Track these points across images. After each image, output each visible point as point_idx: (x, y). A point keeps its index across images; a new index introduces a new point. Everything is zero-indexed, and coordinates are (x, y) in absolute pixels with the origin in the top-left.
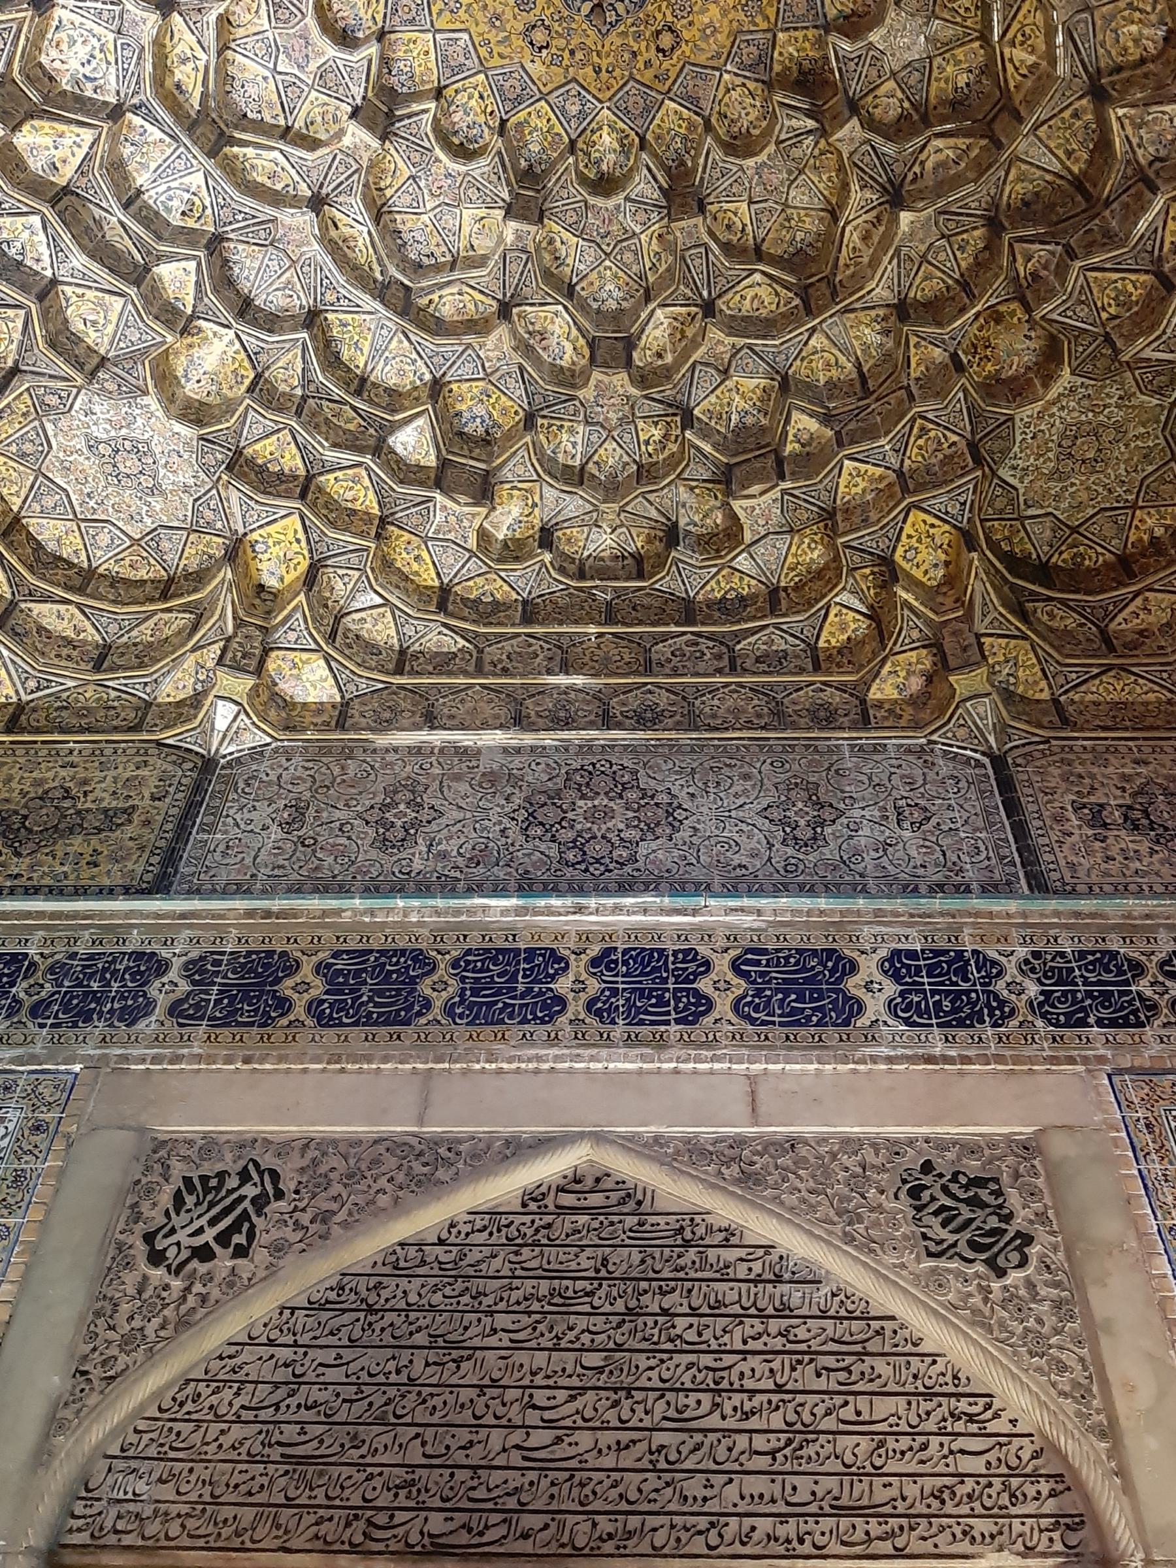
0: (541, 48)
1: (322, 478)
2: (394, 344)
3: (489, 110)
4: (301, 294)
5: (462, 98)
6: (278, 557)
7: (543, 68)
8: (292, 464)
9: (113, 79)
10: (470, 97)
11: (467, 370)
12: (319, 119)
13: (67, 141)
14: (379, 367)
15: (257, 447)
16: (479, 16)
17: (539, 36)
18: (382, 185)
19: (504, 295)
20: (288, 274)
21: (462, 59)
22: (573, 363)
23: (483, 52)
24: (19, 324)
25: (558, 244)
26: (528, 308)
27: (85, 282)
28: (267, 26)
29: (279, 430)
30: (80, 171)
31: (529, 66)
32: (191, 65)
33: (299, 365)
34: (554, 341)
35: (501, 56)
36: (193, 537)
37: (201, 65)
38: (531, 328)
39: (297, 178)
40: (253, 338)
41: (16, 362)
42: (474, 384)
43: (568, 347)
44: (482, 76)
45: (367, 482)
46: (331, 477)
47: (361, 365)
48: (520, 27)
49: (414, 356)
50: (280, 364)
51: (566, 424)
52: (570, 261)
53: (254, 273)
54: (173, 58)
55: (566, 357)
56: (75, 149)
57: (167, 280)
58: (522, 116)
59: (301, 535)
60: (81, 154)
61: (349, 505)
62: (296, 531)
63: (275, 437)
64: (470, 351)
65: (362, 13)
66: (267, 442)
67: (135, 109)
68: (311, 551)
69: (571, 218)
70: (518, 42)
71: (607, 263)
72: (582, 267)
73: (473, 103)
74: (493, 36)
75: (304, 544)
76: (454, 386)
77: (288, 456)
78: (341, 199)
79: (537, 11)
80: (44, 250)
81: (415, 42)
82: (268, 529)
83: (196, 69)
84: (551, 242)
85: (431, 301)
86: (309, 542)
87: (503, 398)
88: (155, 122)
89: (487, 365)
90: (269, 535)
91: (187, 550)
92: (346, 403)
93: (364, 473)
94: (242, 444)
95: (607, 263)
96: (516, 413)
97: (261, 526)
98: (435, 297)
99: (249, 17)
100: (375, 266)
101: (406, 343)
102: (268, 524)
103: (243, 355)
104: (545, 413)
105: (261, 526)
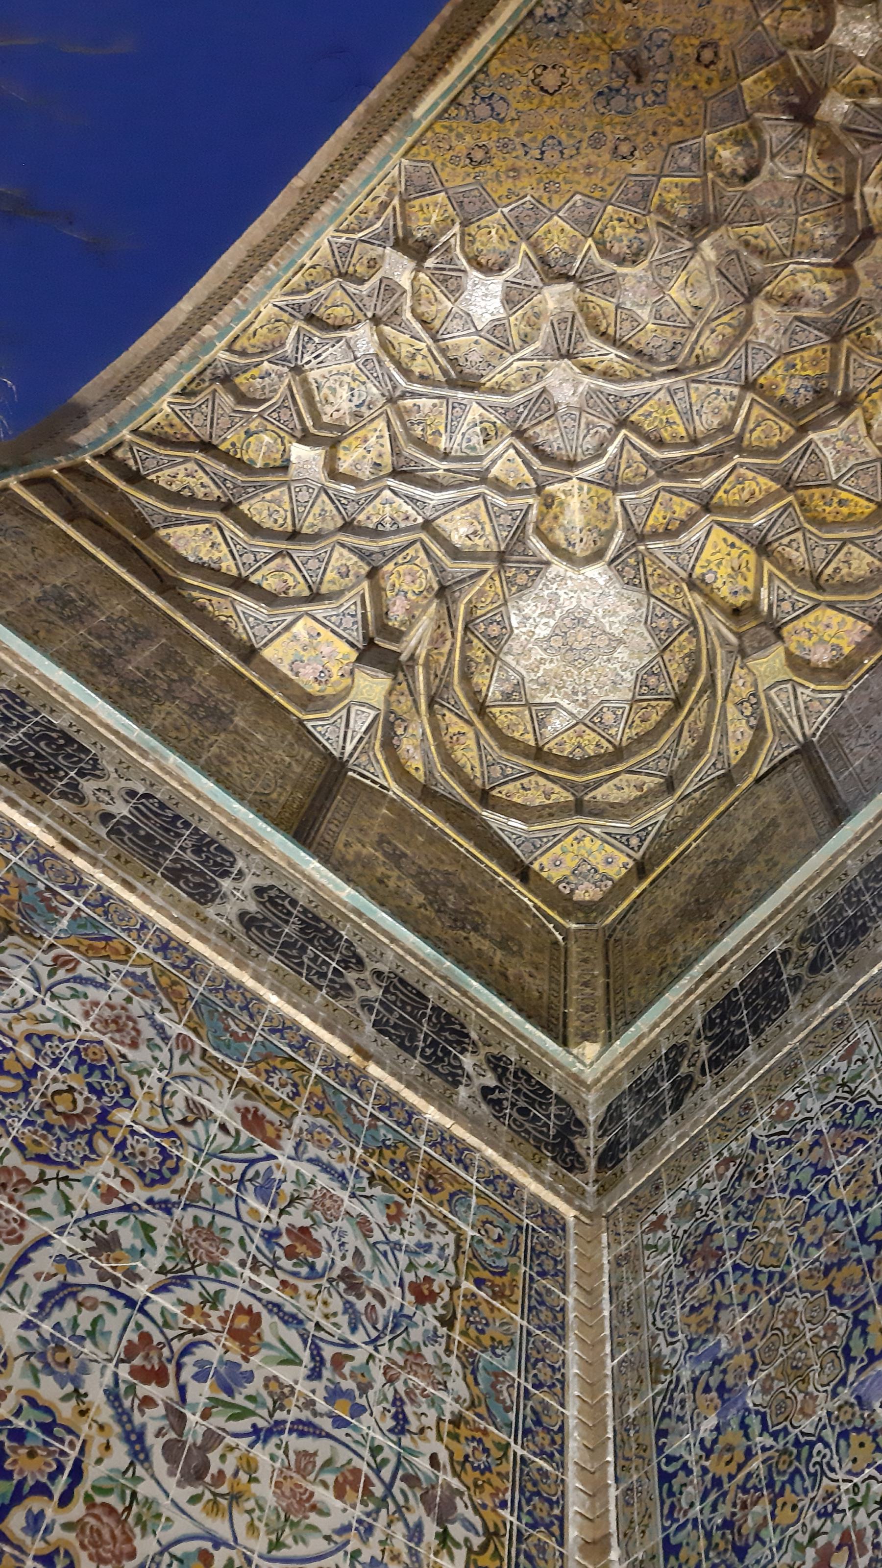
0: (632, 154)
1: (715, 500)
2: (694, 396)
3: (632, 221)
4: (602, 423)
5: (609, 233)
6: (729, 576)
7: (644, 163)
8: (685, 509)
9: (374, 390)
10: (614, 229)
11: (761, 361)
12: (528, 329)
13: (373, 440)
14: (697, 422)
15: (651, 522)
16: (577, 177)
17: (624, 149)
18: (602, 329)
19: (743, 294)
20: (583, 421)
21: (588, 212)
22: (838, 293)
23: (597, 194)
24: (422, 554)
25: (753, 241)
26: (769, 288)
27: (449, 507)
28: (450, 305)
29: (656, 498)
30: (396, 452)
31: (634, 170)
32: (419, 358)
33: (636, 455)
34: (808, 294)
35: (611, 184)
36: (667, 656)
37: (425, 352)
38: (783, 300)
39: (540, 363)
40: (590, 471)
41: (439, 582)
42: (775, 367)
43: (824, 287)
44: (610, 208)
45: (750, 475)
46: (721, 493)
47: (684, 434)
48: (607, 157)
49: (714, 388)
50: (623, 467)
51: (871, 324)
52: (772, 245)
53: (560, 441)
54: (405, 360)
55: (829, 294)
56: (381, 441)
57: (502, 478)
58: (656, 200)
59: (731, 538)
60: (386, 441)
61: (752, 501)
62: (725, 540)
63: (657, 504)
64: (750, 346)
65: (503, 248)
66: (654, 513)
67: (403, 396)
68: (747, 542)
69: (746, 213)
70: (614, 166)
71: (801, 219)
72: (785, 240)
73: (619, 230)
74: (596, 179)
75: (738, 543)
76: (762, 380)
77: (677, 508)
78: (579, 348)
79: (610, 137)
80: (407, 508)
81: (549, 232)
82: (705, 555)
83: (424, 357)
84: (747, 244)
85: (697, 357)
86: (740, 537)
87: (805, 354)
88: (421, 395)
89: (772, 345)
90: (709, 562)
91: (670, 669)
92: (692, 457)
93: (742, 471)
94: (639, 531)
95: (801, 219)
96: (824, 351)
97: (697, 559)
98: (698, 351)
99: (434, 308)
100: (639, 371)
101: (701, 386)
102: (700, 553)
103: (594, 487)
104: (845, 330)
105: (697, 559)
